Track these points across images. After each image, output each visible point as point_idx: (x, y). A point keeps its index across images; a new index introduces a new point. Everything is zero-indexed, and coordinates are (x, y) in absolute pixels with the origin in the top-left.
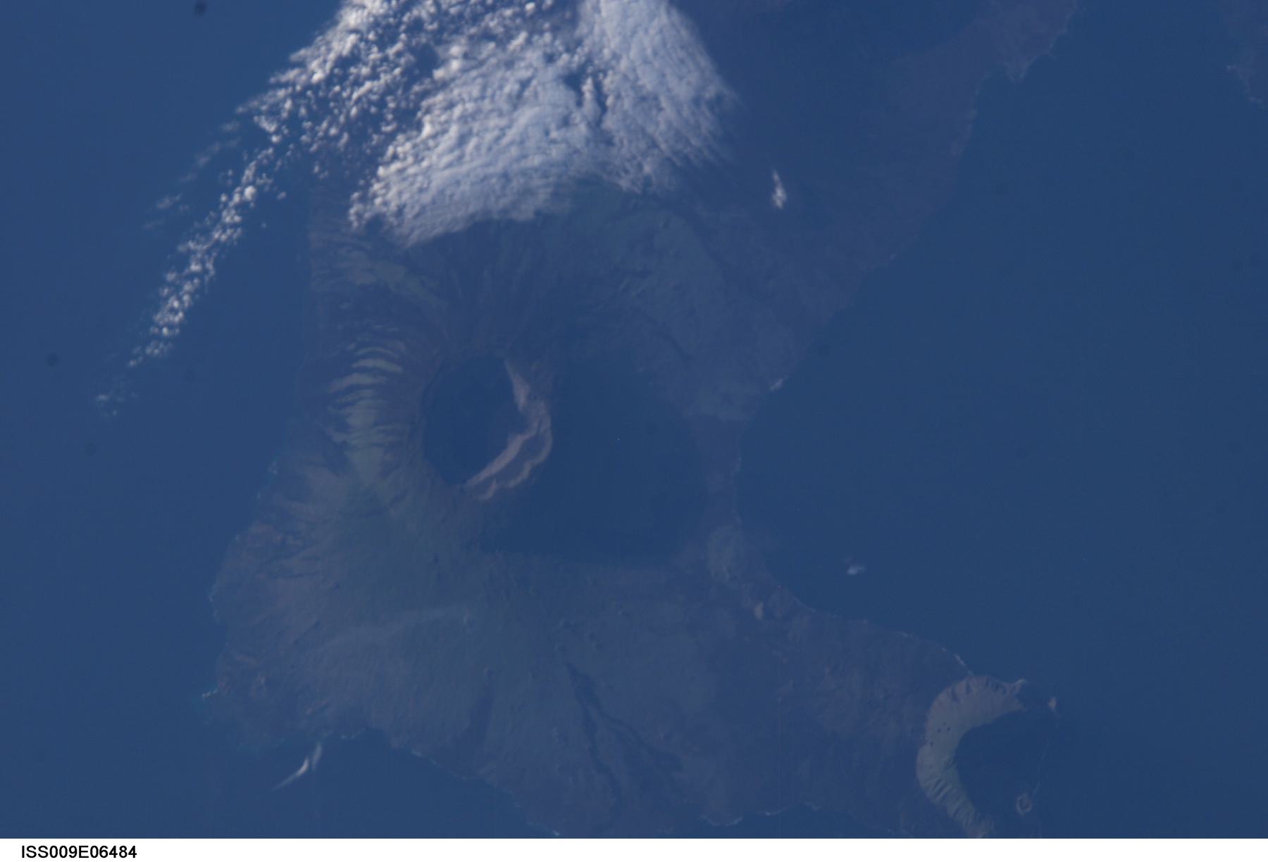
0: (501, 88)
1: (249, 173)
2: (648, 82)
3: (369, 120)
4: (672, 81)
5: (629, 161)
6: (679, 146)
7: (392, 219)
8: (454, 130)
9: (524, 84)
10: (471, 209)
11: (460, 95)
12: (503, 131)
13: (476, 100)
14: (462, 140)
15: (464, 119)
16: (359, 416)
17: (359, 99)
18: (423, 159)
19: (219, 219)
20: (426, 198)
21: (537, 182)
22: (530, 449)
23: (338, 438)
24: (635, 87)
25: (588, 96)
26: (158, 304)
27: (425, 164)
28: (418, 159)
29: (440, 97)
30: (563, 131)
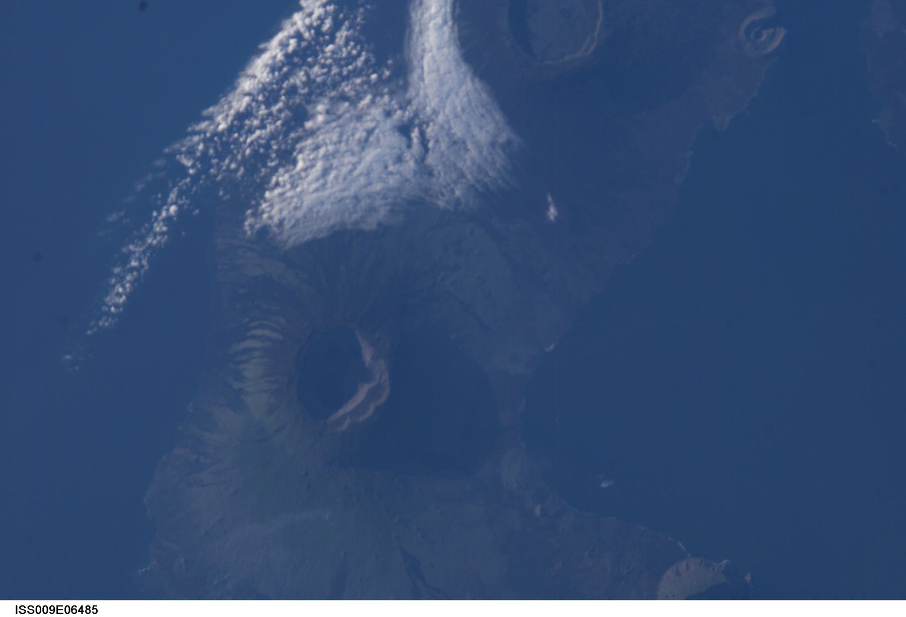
0: (353, 135)
1: (173, 196)
2: (458, 130)
3: (259, 157)
4: (475, 130)
5: (445, 187)
6: (481, 177)
7: (275, 229)
8: (319, 165)
9: (370, 132)
10: (332, 222)
11: (323, 140)
12: (355, 166)
13: (335, 144)
14: (325, 172)
15: (326, 157)
16: (252, 370)
17: (252, 143)
18: (297, 186)
19: (151, 228)
20: (299, 214)
21: (379, 202)
22: (373, 394)
23: (237, 386)
24: (449, 134)
26: (110, 288)
27: (299, 189)
28: (294, 186)
29: (309, 142)
30: (397, 166)
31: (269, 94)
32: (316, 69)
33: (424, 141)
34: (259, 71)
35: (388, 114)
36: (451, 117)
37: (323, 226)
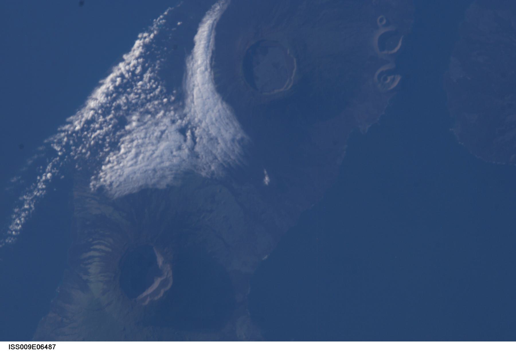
0: (153, 134)
1: (49, 168)
2: (213, 132)
3: (99, 146)
4: (223, 132)
5: (205, 164)
6: (226, 159)
7: (107, 188)
8: (133, 151)
9: (163, 132)
10: (140, 184)
11: (136, 136)
12: (154, 152)
13: (143, 139)
14: (137, 155)
15: (137, 146)
16: (94, 269)
17: (95, 138)
18: (120, 163)
19: (36, 186)
20: (122, 179)
21: (167, 173)
22: (163, 284)
23: (85, 277)
24: (208, 134)
25: (189, 137)
27: (121, 165)
28: (119, 163)
29: (128, 137)
30: (178, 152)
31: (105, 109)
32: (132, 95)
34: (99, 96)
35: (173, 122)
36: (209, 124)
37: (136, 186)
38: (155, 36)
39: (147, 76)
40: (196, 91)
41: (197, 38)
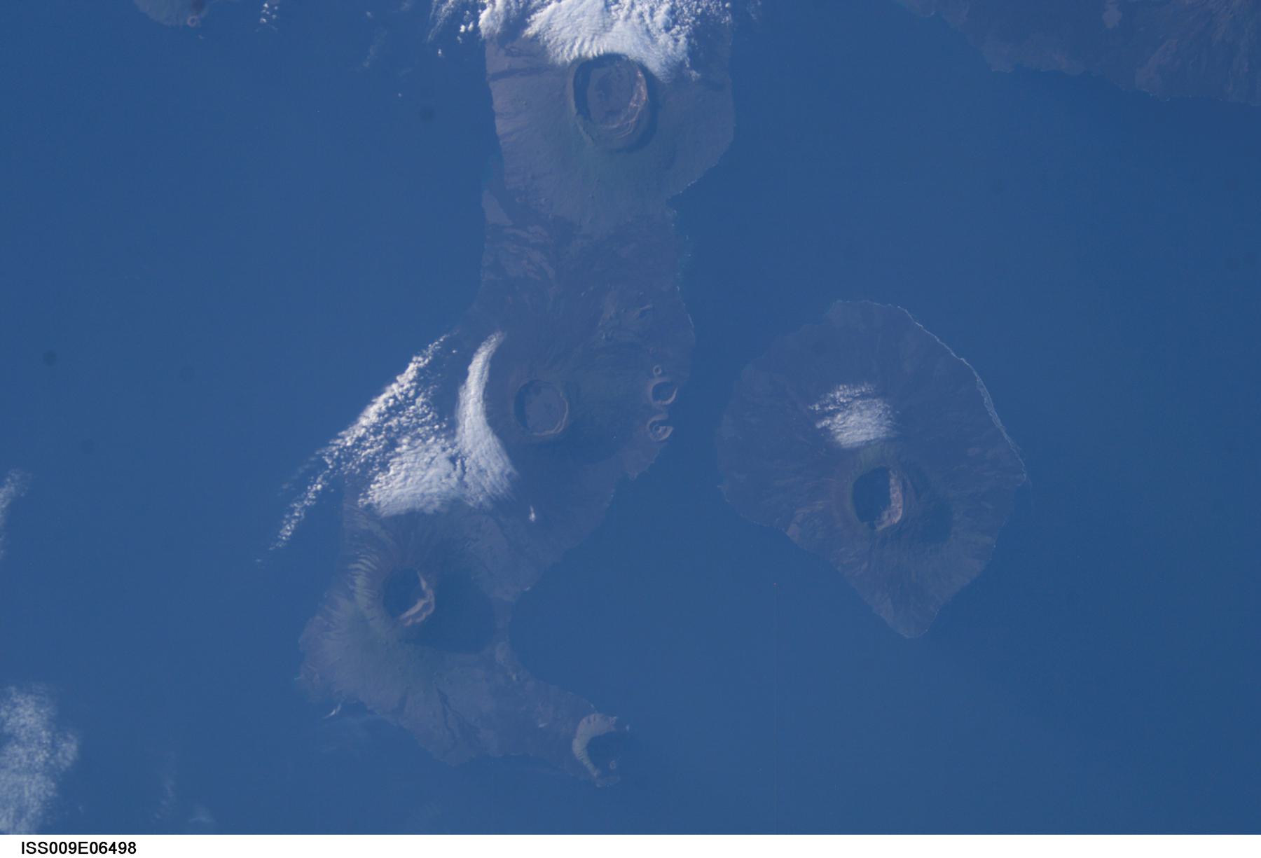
1: (319, 479)
2: (483, 464)
3: (368, 464)
4: (492, 465)
8: (403, 474)
9: (433, 459)
12: (423, 477)
14: (406, 478)
15: (407, 470)
16: (360, 581)
20: (390, 500)
21: (435, 499)
22: (426, 607)
23: (351, 587)
25: (459, 467)
26: (281, 526)
28: (387, 483)
29: (397, 459)
31: (376, 429)
32: (403, 419)
33: (463, 468)
34: (371, 415)
35: (444, 449)
38: (430, 362)
39: (419, 400)
40: (467, 422)
41: (471, 368)
